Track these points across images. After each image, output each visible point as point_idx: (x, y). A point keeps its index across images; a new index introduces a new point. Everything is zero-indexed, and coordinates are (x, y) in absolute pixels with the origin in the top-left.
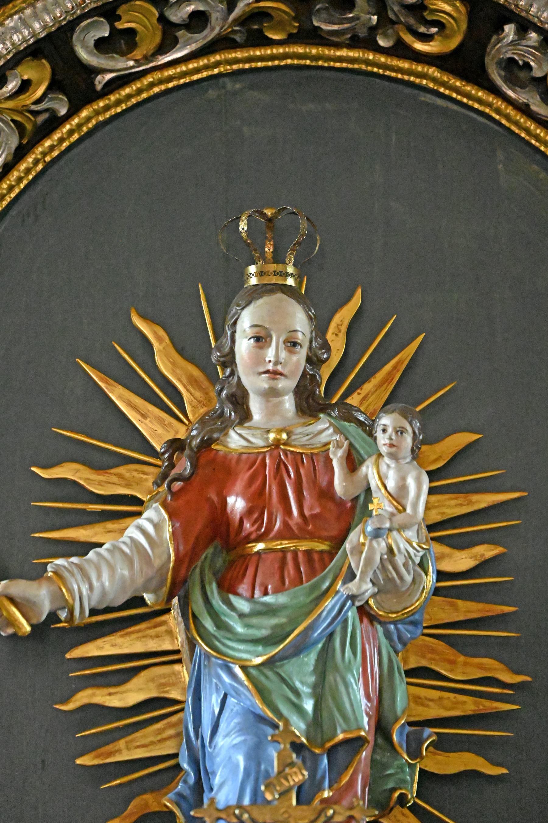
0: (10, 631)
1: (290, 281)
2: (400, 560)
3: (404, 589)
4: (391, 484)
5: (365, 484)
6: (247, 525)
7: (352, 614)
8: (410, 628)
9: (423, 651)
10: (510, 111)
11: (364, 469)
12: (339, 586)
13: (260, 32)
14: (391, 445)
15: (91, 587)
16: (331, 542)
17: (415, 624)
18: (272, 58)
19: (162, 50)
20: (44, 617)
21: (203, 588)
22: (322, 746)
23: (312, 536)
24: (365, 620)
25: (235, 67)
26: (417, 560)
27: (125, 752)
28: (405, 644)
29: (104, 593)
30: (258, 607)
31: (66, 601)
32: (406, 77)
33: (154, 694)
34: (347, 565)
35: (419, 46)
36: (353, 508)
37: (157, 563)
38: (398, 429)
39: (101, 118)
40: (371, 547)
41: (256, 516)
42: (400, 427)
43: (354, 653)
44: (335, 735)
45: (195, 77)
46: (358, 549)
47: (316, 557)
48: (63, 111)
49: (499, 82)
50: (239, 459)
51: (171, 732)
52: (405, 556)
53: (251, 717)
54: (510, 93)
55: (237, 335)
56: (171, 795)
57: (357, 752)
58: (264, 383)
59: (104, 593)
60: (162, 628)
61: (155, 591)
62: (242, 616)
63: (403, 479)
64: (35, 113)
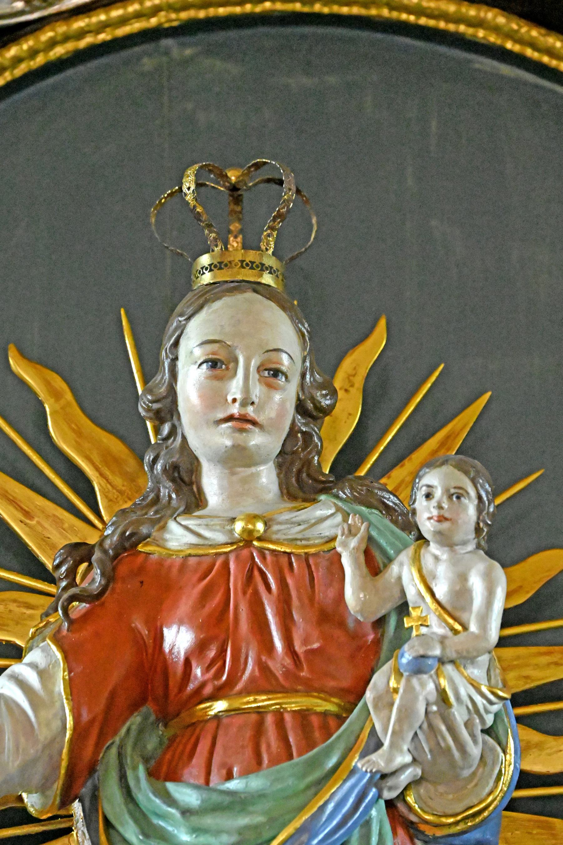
3: (466, 773)
5: (396, 593)
6: (198, 671)
11: (395, 568)
12: (356, 761)
14: (441, 519)
16: (340, 697)
21: (123, 777)
24: (401, 832)
25: (184, 15)
26: (489, 720)
30: (215, 798)
32: (452, 27)
34: (369, 730)
36: (378, 642)
38: (452, 491)
40: (409, 689)
41: (212, 653)
42: (455, 488)
47: (315, 720)
50: (183, 567)
52: (468, 708)
55: (180, 364)
61: (42, 789)
62: (186, 812)
63: (463, 578)
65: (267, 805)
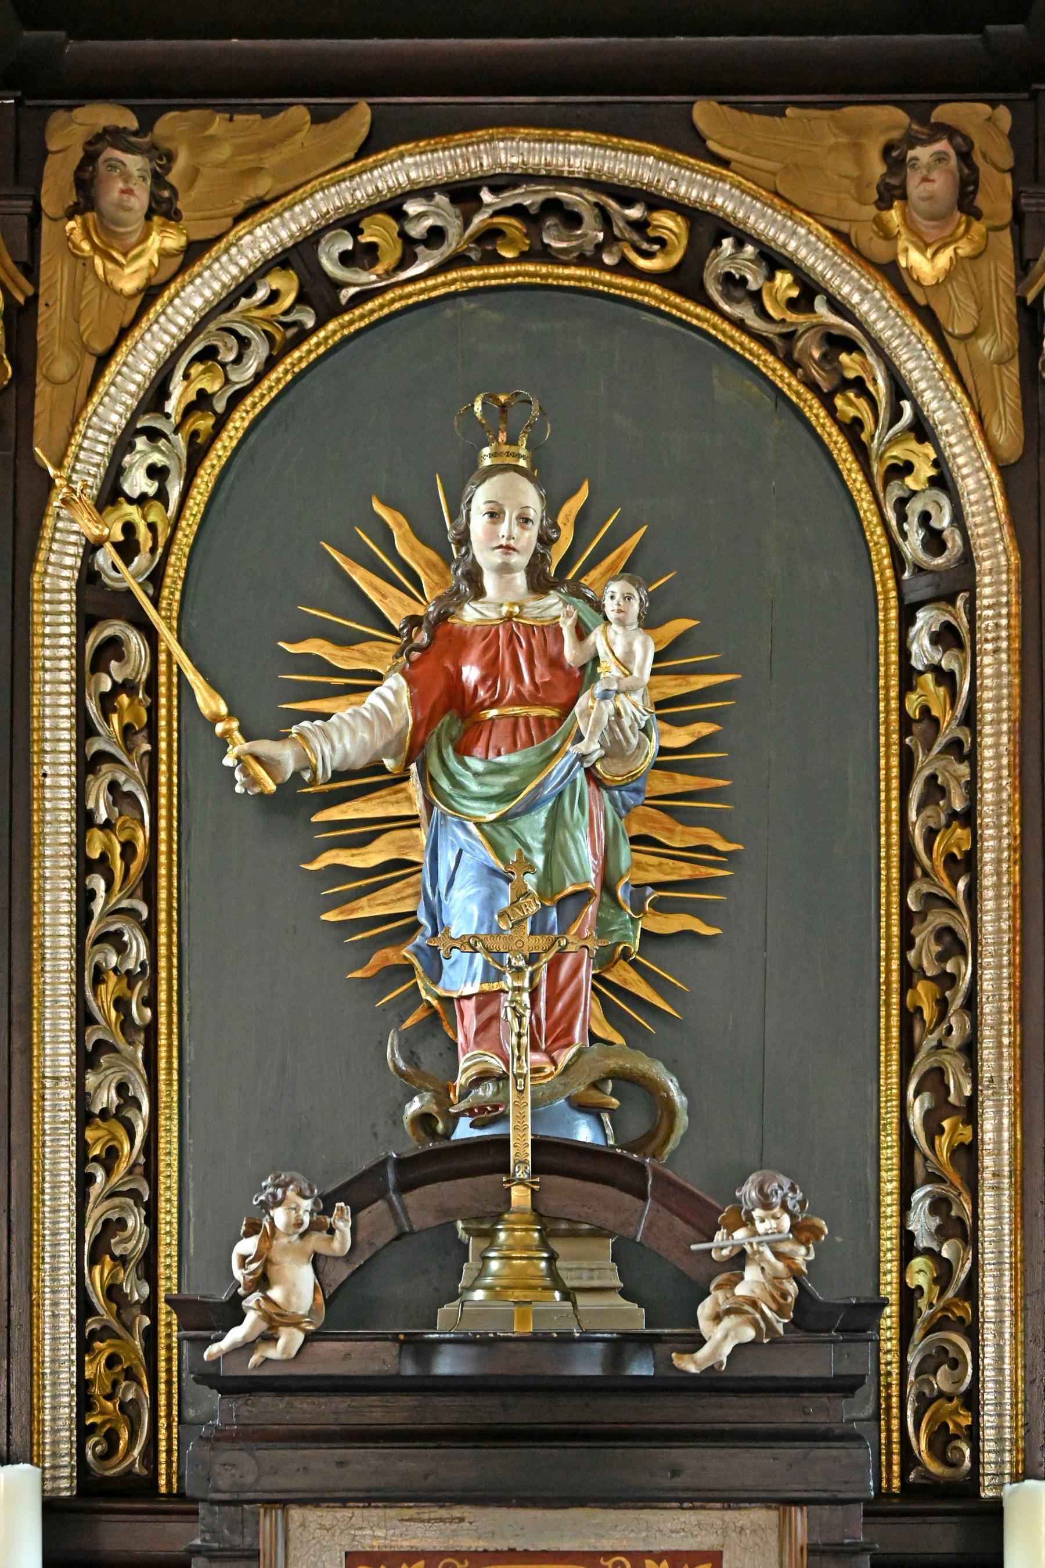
0: (257, 790)
1: (522, 463)
2: (626, 722)
4: (619, 651)
5: (593, 651)
6: (481, 693)
7: (580, 776)
8: (633, 795)
9: (645, 820)
10: (726, 326)
11: (592, 638)
12: (568, 747)
13: (495, 251)
14: (619, 611)
15: (333, 748)
17: (637, 791)
18: (505, 276)
19: (403, 264)
20: (288, 776)
22: (551, 899)
23: (543, 703)
25: (471, 284)
26: (643, 724)
27: (367, 909)
28: (628, 810)
29: (346, 755)
30: (492, 767)
31: (309, 760)
32: (629, 295)
33: (394, 856)
35: (642, 263)
36: (581, 677)
37: (396, 727)
39: (346, 332)
40: (600, 708)
41: (489, 683)
43: (583, 813)
44: (564, 888)
45: (434, 294)
46: (586, 713)
47: (546, 722)
48: (310, 323)
49: (716, 297)
50: (473, 632)
51: (410, 891)
53: (485, 871)
54: (726, 308)
55: (472, 513)
56: (410, 947)
57: (586, 904)
58: (497, 557)
59: (346, 755)
60: (401, 795)
61: (394, 757)
62: (476, 774)
63: (630, 644)
64: (286, 326)
65: (520, 771)
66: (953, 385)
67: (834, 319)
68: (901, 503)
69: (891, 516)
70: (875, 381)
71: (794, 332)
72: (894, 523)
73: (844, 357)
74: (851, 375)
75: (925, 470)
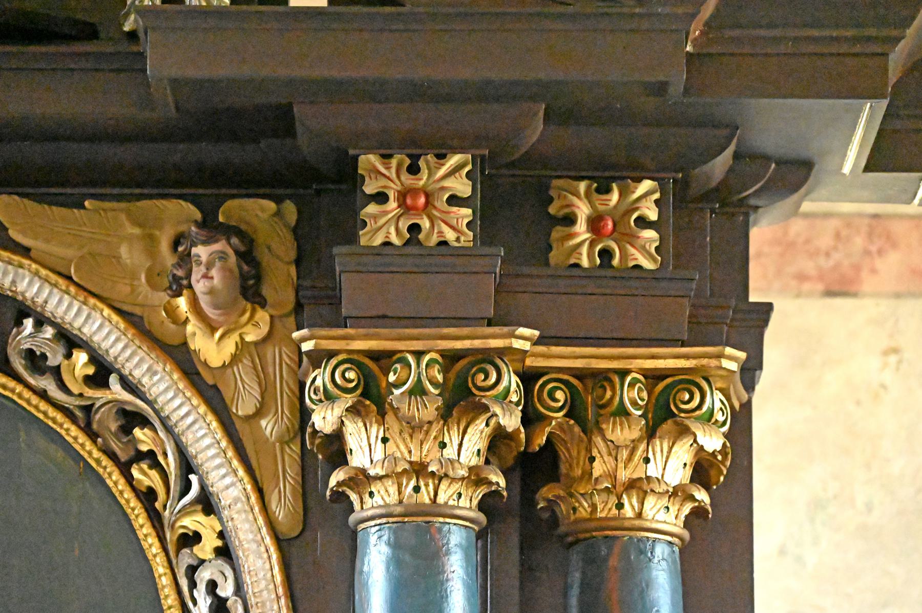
54: (31, 381)
66: (235, 463)
67: (126, 396)
68: (192, 570)
69: (184, 583)
70: (165, 455)
71: (92, 405)
72: (185, 589)
73: (137, 432)
74: (144, 448)
75: (210, 542)
